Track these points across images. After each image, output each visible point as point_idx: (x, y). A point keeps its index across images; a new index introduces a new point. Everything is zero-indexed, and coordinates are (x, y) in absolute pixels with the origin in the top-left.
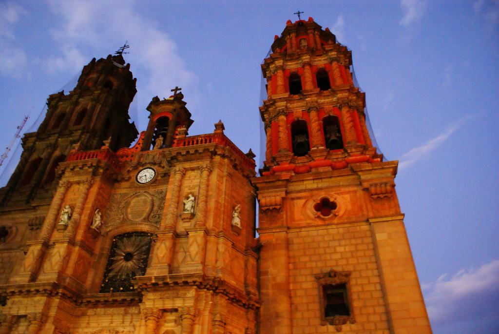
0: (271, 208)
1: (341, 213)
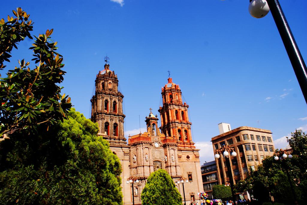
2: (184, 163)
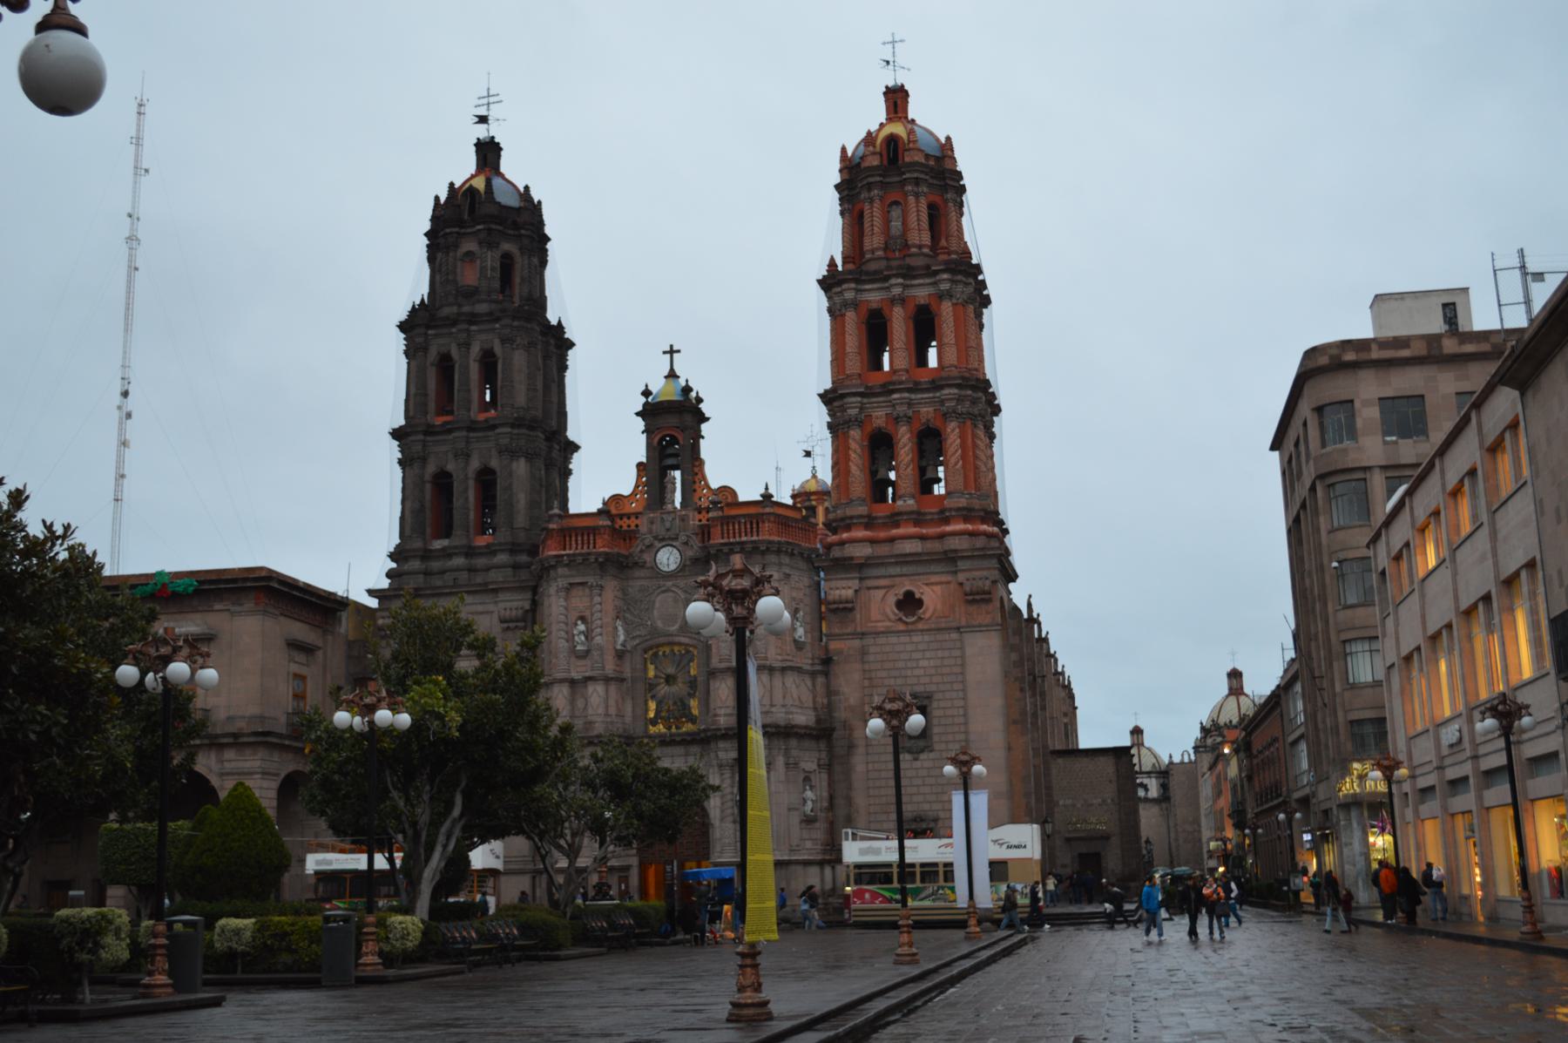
0: (841, 606)
2: (882, 640)
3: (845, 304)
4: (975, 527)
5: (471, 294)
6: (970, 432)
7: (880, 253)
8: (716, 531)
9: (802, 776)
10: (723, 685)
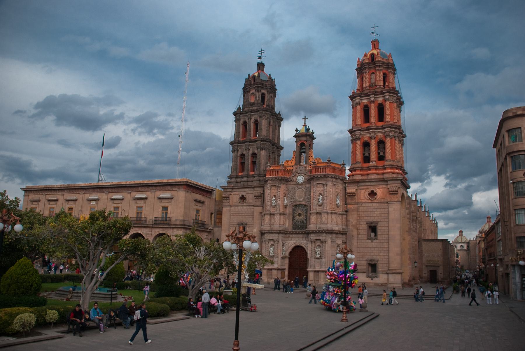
0: (351, 194)
1: (378, 198)
2: (363, 205)
3: (357, 104)
4: (394, 171)
5: (252, 104)
6: (394, 141)
7: (368, 88)
8: (314, 171)
9: (336, 246)
10: (313, 217)
